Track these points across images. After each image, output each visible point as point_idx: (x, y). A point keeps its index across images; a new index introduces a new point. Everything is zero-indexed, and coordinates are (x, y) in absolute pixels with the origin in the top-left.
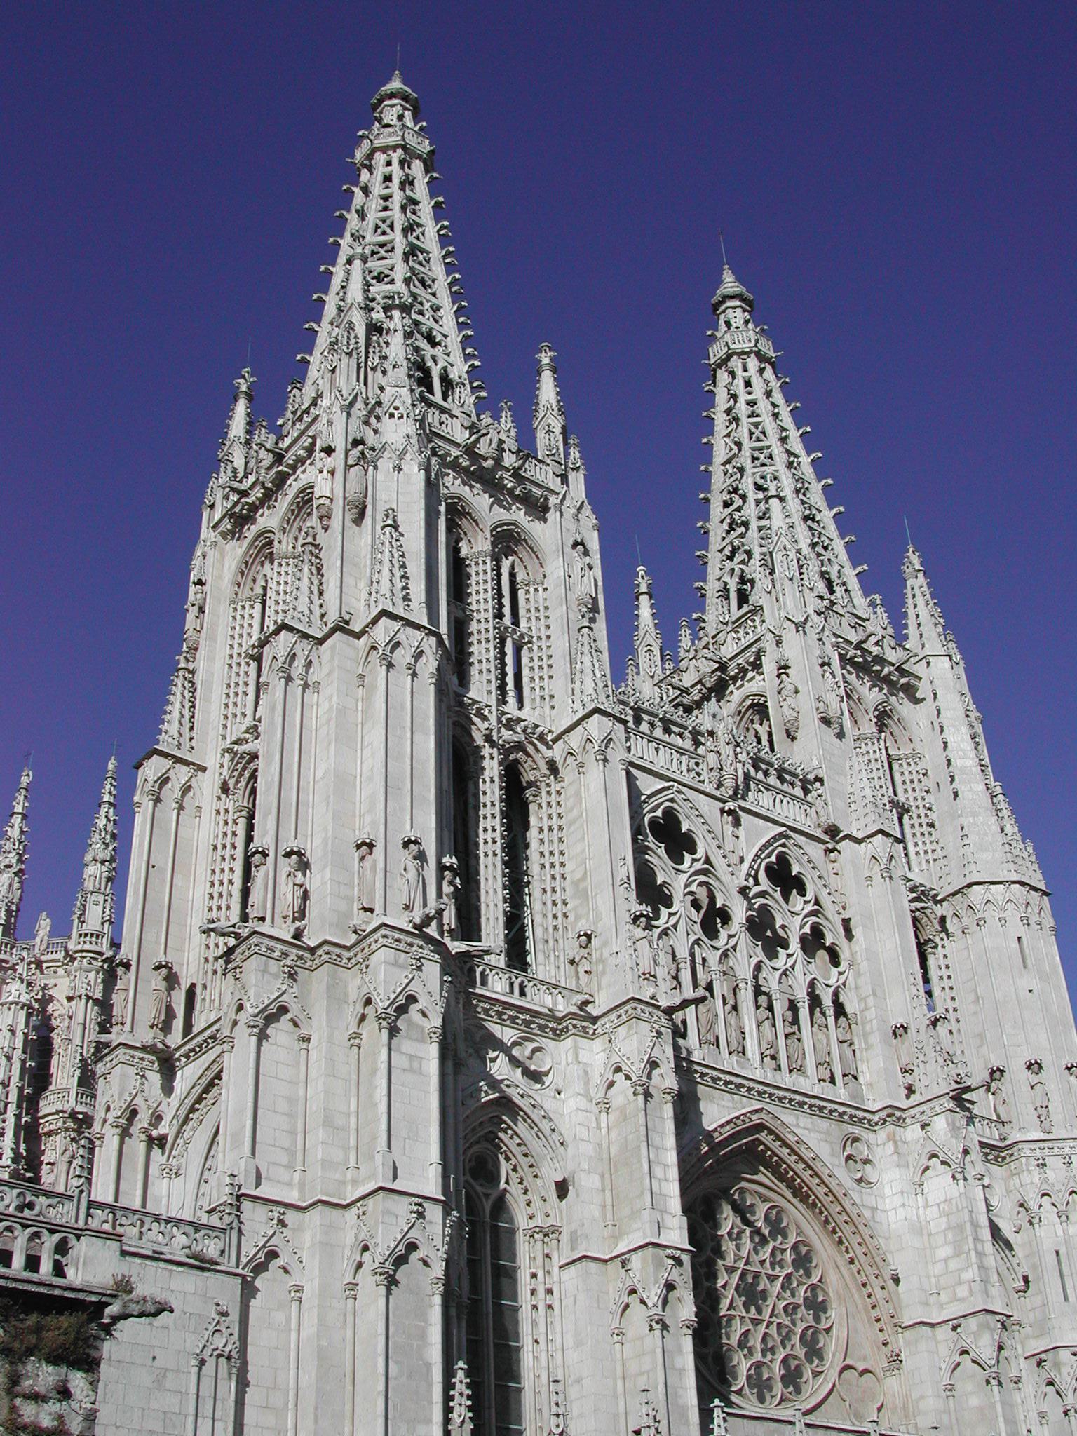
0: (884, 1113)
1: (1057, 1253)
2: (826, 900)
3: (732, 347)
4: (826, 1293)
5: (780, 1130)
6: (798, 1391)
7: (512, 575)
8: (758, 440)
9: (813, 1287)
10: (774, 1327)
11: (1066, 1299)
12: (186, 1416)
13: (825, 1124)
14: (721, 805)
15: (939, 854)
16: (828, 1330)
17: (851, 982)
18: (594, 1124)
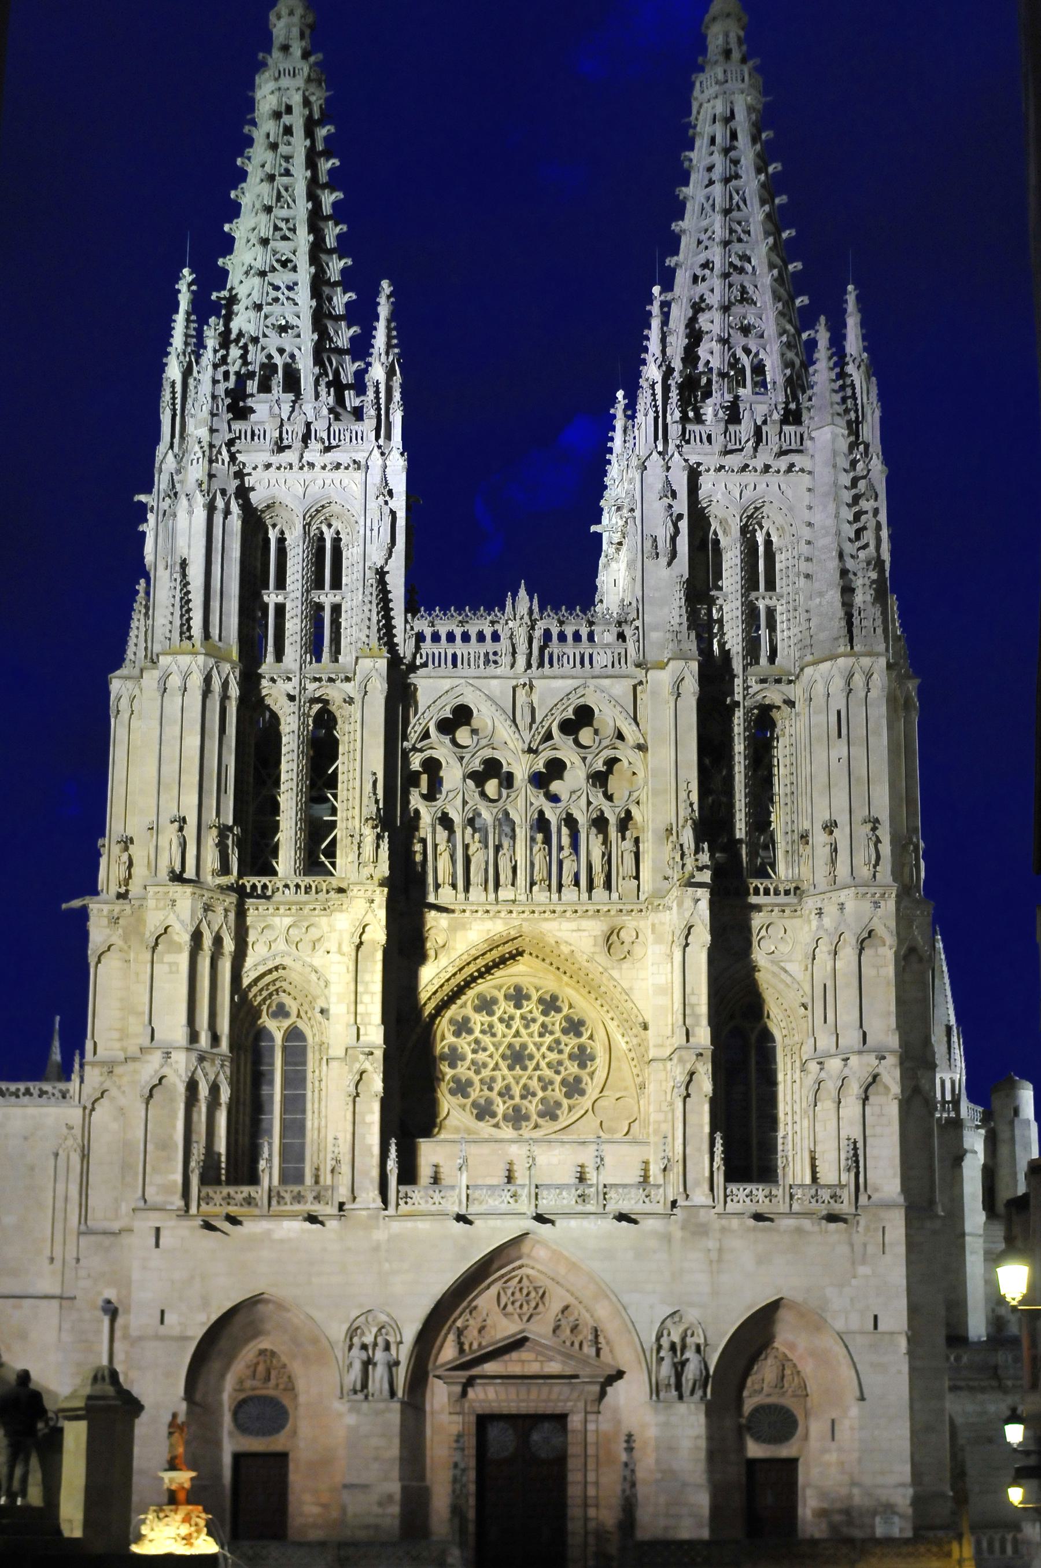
10: (535, 1079)
16: (592, 1075)
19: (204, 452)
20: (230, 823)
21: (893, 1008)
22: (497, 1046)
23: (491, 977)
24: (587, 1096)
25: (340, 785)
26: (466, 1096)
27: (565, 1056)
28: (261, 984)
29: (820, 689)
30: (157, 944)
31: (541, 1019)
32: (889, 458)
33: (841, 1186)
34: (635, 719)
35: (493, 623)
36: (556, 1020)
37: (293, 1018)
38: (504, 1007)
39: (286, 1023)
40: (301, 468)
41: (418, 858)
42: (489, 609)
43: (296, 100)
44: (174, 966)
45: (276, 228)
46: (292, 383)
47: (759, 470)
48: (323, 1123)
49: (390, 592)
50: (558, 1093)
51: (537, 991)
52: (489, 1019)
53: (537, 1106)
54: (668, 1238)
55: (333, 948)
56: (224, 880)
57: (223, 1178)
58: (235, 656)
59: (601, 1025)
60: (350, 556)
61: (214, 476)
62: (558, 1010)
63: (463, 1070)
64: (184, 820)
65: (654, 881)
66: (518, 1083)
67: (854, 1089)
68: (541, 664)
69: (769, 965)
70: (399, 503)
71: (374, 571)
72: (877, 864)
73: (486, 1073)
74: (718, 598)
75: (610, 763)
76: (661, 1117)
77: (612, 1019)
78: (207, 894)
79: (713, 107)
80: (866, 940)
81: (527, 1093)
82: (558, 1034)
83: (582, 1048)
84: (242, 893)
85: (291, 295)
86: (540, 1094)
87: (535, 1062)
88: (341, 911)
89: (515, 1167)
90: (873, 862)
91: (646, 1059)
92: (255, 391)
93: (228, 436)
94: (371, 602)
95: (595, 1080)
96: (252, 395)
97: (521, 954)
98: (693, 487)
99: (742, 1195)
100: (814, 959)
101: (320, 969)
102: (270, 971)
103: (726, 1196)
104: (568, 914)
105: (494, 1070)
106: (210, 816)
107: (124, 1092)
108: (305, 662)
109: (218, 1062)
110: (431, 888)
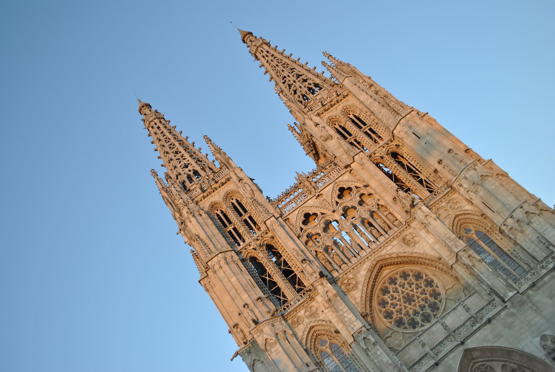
1: (483, 202)
2: (358, 185)
3: (253, 52)
4: (430, 278)
5: (383, 257)
6: (438, 309)
7: (237, 201)
8: (275, 70)
9: (426, 280)
10: (421, 301)
11: (494, 212)
13: (395, 243)
14: (315, 197)
15: (384, 129)
16: (437, 286)
17: (379, 197)
18: (332, 313)
22: (399, 300)
24: (442, 294)
27: (423, 287)
28: (309, 338)
31: (406, 282)
50: (432, 300)
52: (390, 294)
54: (513, 315)
55: (323, 308)
62: (409, 275)
66: (416, 307)
73: (404, 312)
91: (450, 267)
95: (439, 287)
105: (405, 309)
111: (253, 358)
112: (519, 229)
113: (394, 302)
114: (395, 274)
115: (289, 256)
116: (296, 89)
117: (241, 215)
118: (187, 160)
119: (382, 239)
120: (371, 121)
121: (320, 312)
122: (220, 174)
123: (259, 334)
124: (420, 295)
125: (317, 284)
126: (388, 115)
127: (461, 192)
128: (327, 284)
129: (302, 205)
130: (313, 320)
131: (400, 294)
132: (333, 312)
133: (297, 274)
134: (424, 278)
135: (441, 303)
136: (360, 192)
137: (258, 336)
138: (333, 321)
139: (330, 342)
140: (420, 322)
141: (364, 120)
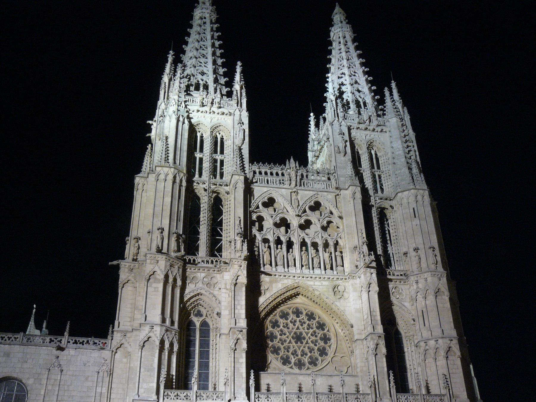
0: (348, 276)
1: (422, 311)
2: (334, 211)
6: (316, 365)
10: (307, 347)
12: (94, 387)
13: (326, 283)
16: (330, 346)
17: (343, 236)
18: (228, 296)
19: (176, 103)
20: (181, 233)
21: (452, 320)
23: (286, 304)
24: (329, 356)
25: (223, 224)
26: (278, 354)
27: (318, 338)
28: (192, 301)
29: (405, 201)
30: (149, 279)
31: (308, 322)
32: (414, 130)
33: (444, 395)
34: (337, 207)
35: (282, 169)
36: (314, 323)
37: (204, 317)
38: (292, 317)
39: (201, 319)
40: (210, 113)
41: (256, 253)
42: (280, 165)
43: (207, 16)
44: (156, 289)
45: (201, 47)
46: (206, 87)
47: (371, 130)
48: (217, 364)
49: (243, 155)
50: (316, 354)
51: (305, 311)
52: (286, 321)
53: (308, 360)
55: (223, 287)
56: (179, 254)
57: (174, 386)
58: (185, 172)
59: (332, 325)
60: (227, 144)
61: (179, 110)
62: (314, 319)
63: (276, 343)
64: (163, 229)
65: (351, 267)
66: (299, 349)
67: (442, 353)
68: (301, 185)
69: (397, 303)
70: (246, 127)
71: (238, 147)
72: (436, 264)
73: (286, 344)
74: (361, 170)
75: (329, 222)
76: (363, 364)
77: (337, 323)
78: (171, 260)
79: (339, 35)
80: (437, 292)
81: (304, 354)
82: (315, 329)
83: (325, 335)
84: (186, 263)
85: (206, 65)
86: (309, 354)
87: (306, 340)
88: (226, 272)
89: (302, 386)
90: (435, 263)
92: (193, 90)
93: (184, 100)
94: (237, 157)
96: (192, 91)
97: (298, 294)
98: (350, 134)
99: (403, 398)
100: (417, 300)
101: (216, 295)
102: (195, 296)
103: (397, 399)
104: (317, 279)
105: (289, 343)
106: (174, 229)
107: (130, 345)
108: (210, 178)
109: (174, 332)
110: (262, 265)
111: (130, 278)
112: (433, 355)
113: (285, 331)
114: (304, 309)
115: (228, 220)
116: (345, 92)
117: (216, 152)
118: (207, 69)
119: (317, 271)
120: (386, 169)
121: (217, 288)
122: (227, 104)
123: (153, 262)
124: (310, 342)
125: (236, 263)
126: (405, 177)
127: (412, 288)
128: (243, 269)
129: (274, 188)
130: (207, 289)
131: (295, 328)
132: (229, 297)
133: (223, 239)
134: (325, 331)
135: (322, 362)
136: (331, 219)
137: (151, 263)
138: (223, 304)
139: (205, 318)
140: (293, 363)
141: (382, 163)
